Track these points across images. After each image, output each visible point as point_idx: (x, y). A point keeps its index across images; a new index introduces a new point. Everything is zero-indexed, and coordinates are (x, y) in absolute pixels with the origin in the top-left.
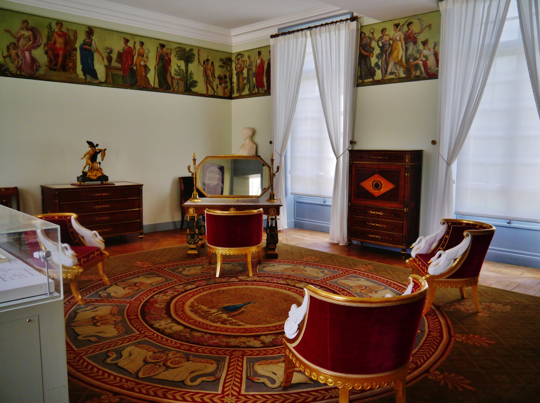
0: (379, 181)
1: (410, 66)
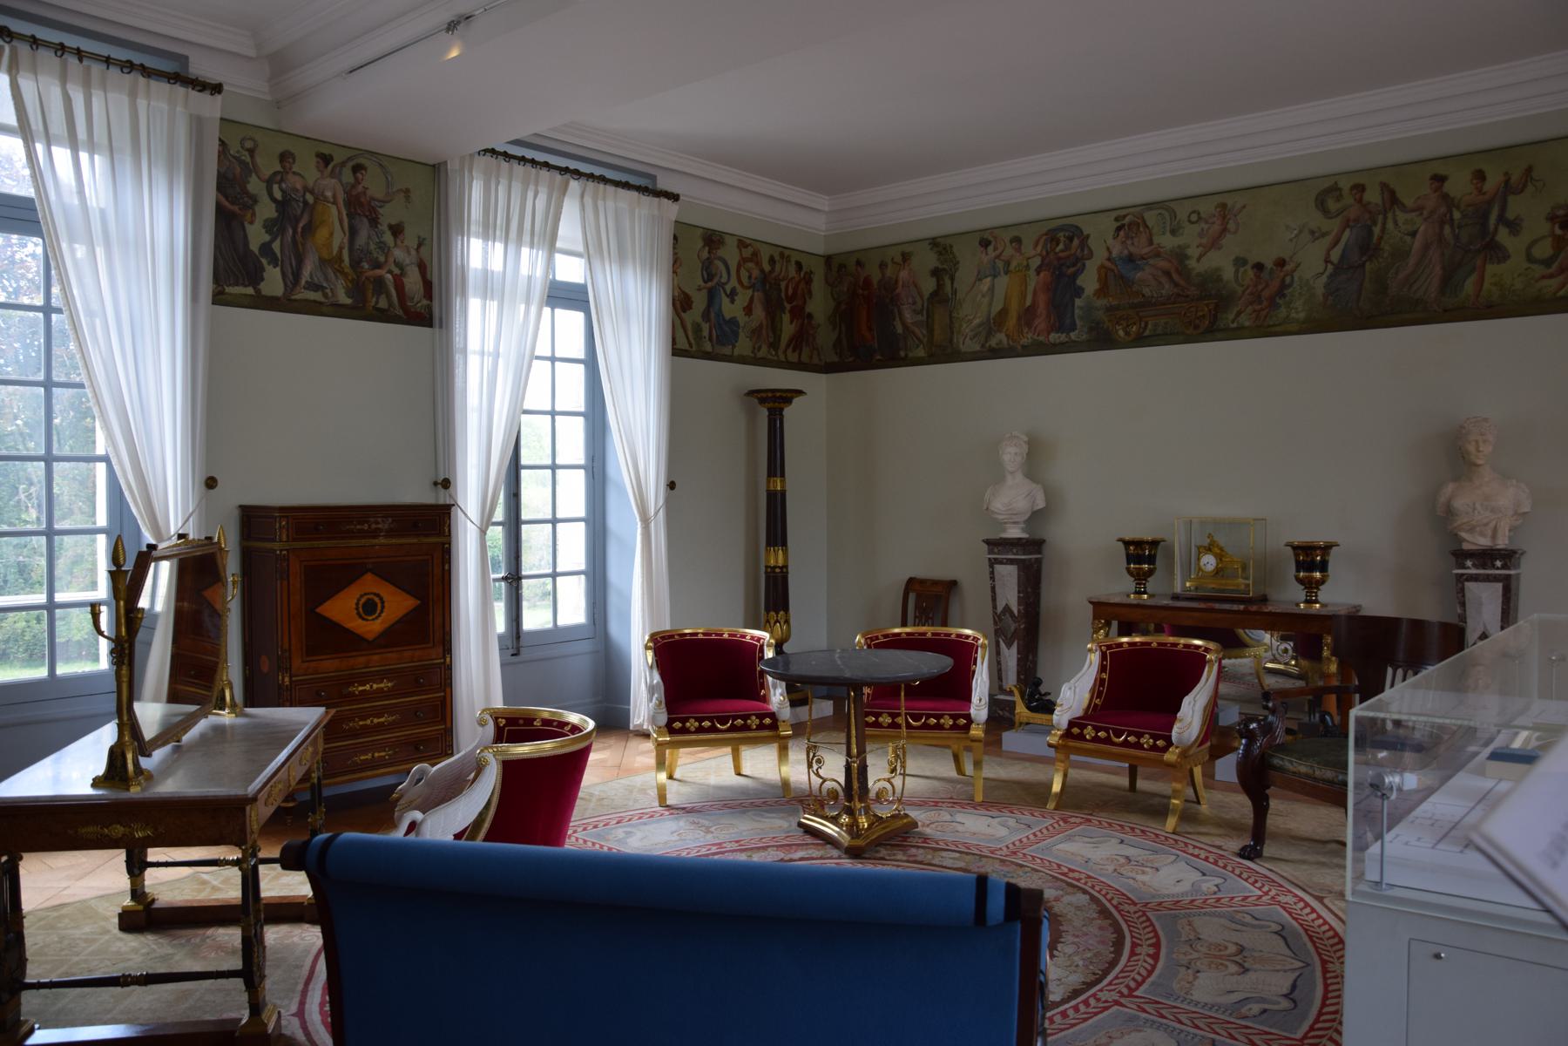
1: (364, 278)
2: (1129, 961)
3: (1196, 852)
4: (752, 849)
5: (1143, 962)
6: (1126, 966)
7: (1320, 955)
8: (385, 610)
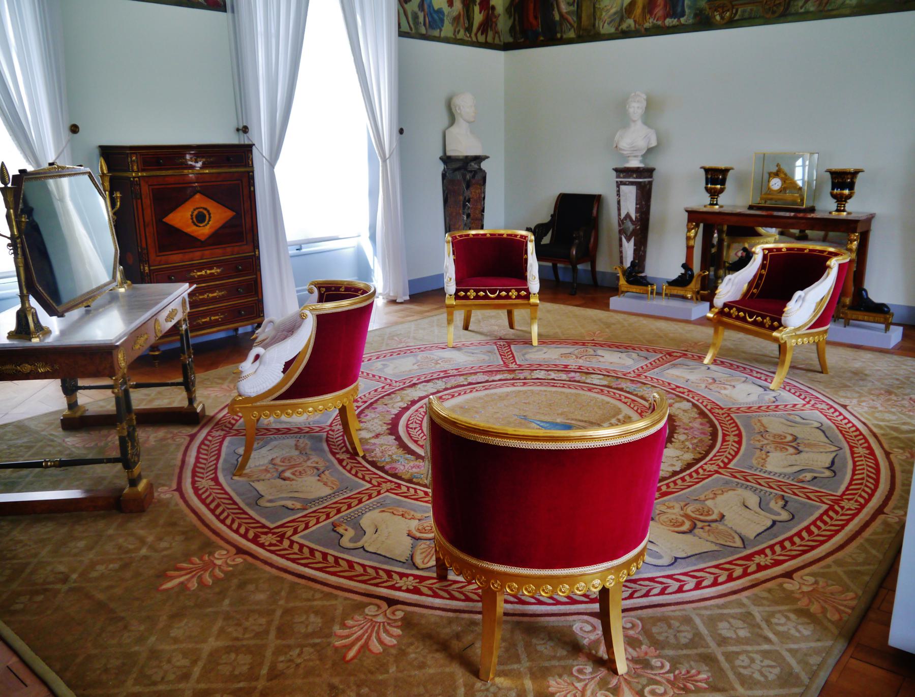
0: (205, 209)
2: (722, 445)
3: (759, 375)
4: (467, 374)
5: (731, 447)
6: (720, 449)
7: (848, 442)
8: (211, 219)
